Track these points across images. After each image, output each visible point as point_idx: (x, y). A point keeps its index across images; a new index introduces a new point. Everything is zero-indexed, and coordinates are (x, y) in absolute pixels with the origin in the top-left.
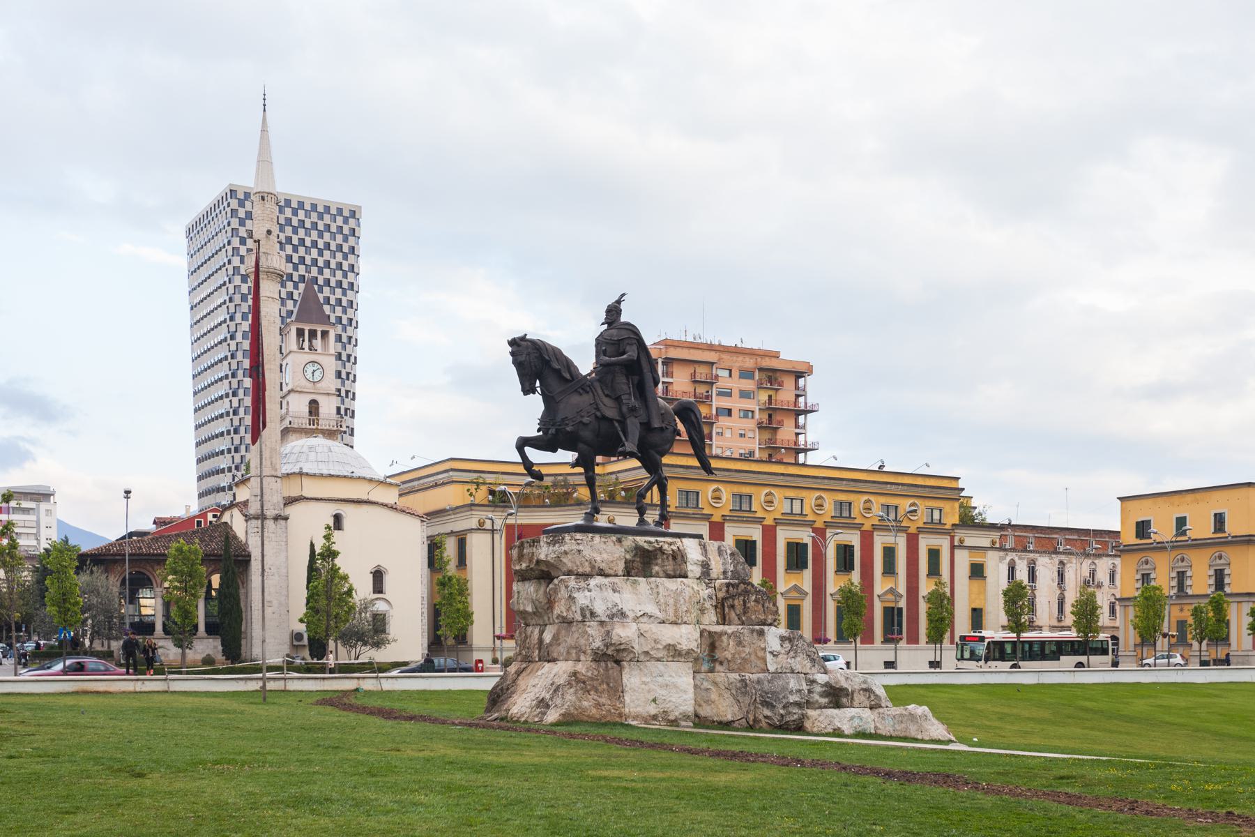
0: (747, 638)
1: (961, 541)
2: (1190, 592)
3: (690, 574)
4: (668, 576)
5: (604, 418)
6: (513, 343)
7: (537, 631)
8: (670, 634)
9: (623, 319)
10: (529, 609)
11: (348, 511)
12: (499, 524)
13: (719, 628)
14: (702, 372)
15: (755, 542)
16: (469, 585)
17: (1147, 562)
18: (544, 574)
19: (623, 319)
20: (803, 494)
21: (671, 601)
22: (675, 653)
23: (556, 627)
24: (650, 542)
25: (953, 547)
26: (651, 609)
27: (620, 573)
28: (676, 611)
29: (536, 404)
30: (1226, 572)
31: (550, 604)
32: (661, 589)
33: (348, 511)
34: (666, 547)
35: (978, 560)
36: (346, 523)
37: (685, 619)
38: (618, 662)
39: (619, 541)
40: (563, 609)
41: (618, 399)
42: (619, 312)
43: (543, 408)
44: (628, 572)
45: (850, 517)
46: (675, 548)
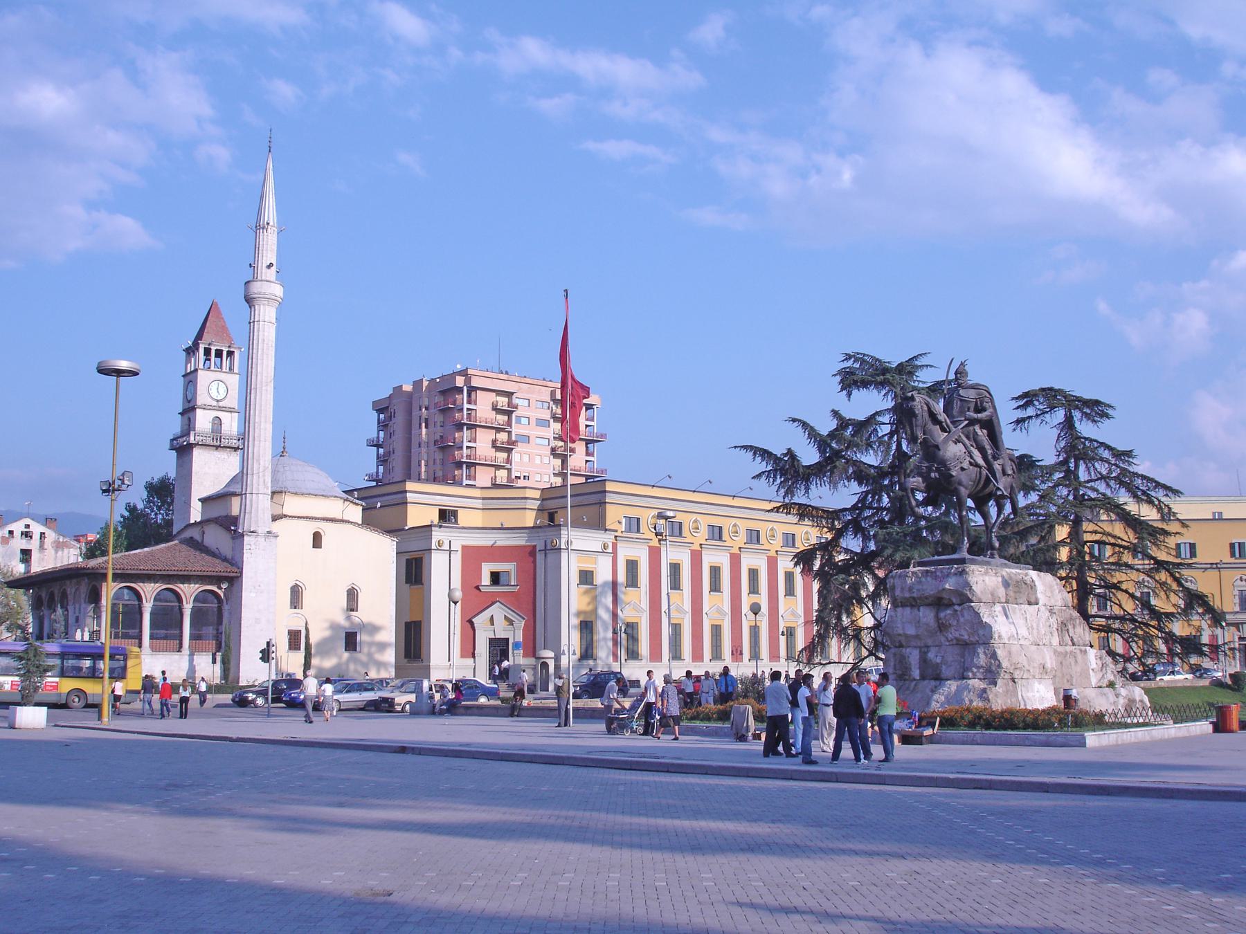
0: (1079, 656)
4: (1030, 604)
5: (974, 464)
11: (327, 530)
12: (457, 546)
13: (1061, 649)
14: (503, 402)
31: (942, 627)
41: (982, 450)
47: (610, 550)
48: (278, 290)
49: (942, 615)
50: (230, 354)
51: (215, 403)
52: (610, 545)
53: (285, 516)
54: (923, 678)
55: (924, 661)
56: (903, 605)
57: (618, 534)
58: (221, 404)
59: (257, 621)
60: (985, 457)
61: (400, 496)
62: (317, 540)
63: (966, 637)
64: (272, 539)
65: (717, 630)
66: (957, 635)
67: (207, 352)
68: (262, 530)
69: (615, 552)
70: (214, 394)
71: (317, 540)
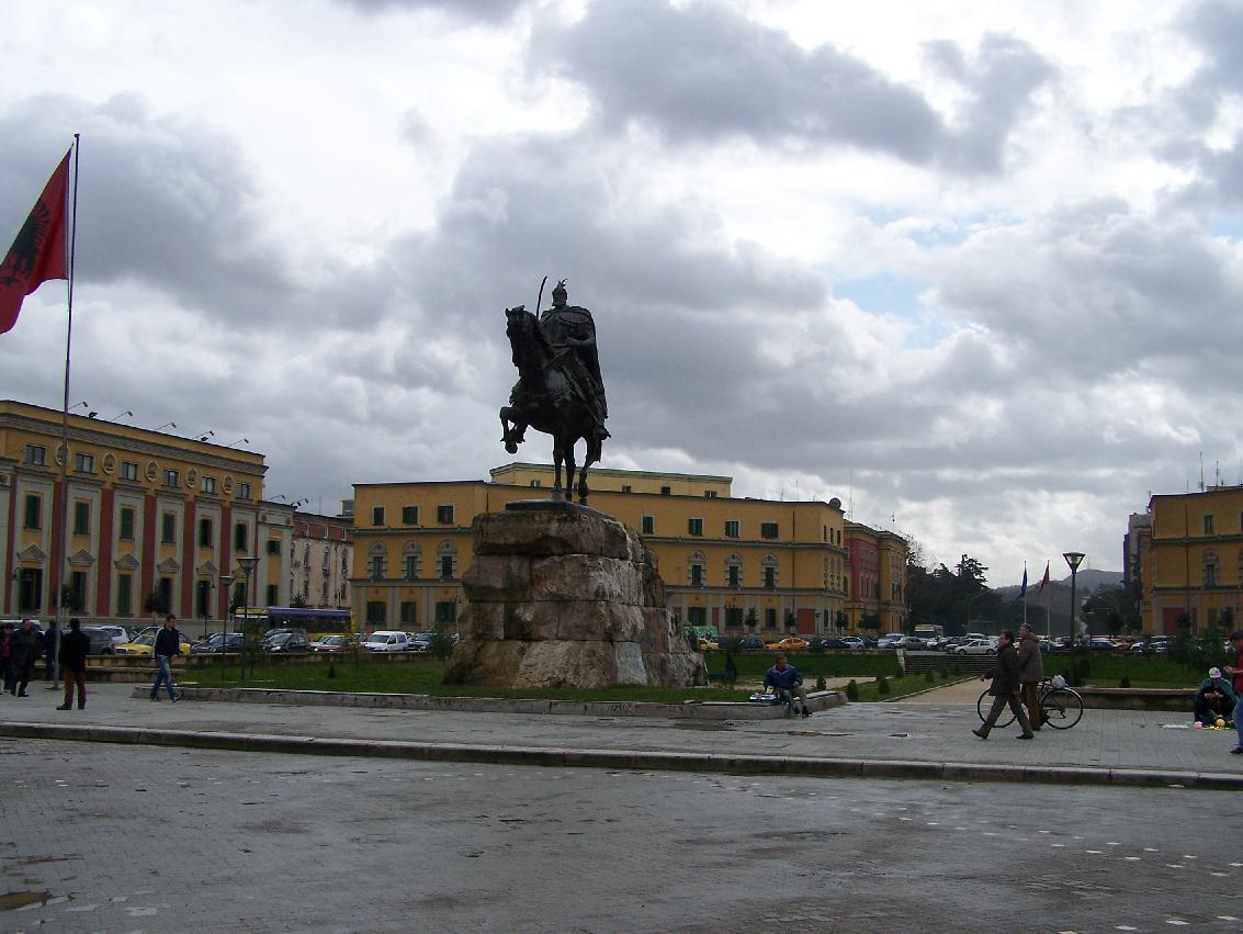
1: (264, 518)
2: (419, 576)
5: (576, 397)
7: (501, 608)
9: (570, 303)
10: (499, 584)
15: (777, 536)
16: (1104, 583)
17: (379, 547)
18: (534, 550)
19: (570, 303)
20: (139, 459)
23: (537, 605)
25: (258, 523)
30: (776, 570)
31: (535, 580)
35: (276, 537)
42: (564, 294)
45: (135, 480)
47: (8, 484)
49: (537, 566)
52: (9, 480)
54: (508, 638)
55: (511, 617)
57: (20, 465)
60: (585, 391)
65: (125, 582)
66: (554, 589)
69: (13, 490)
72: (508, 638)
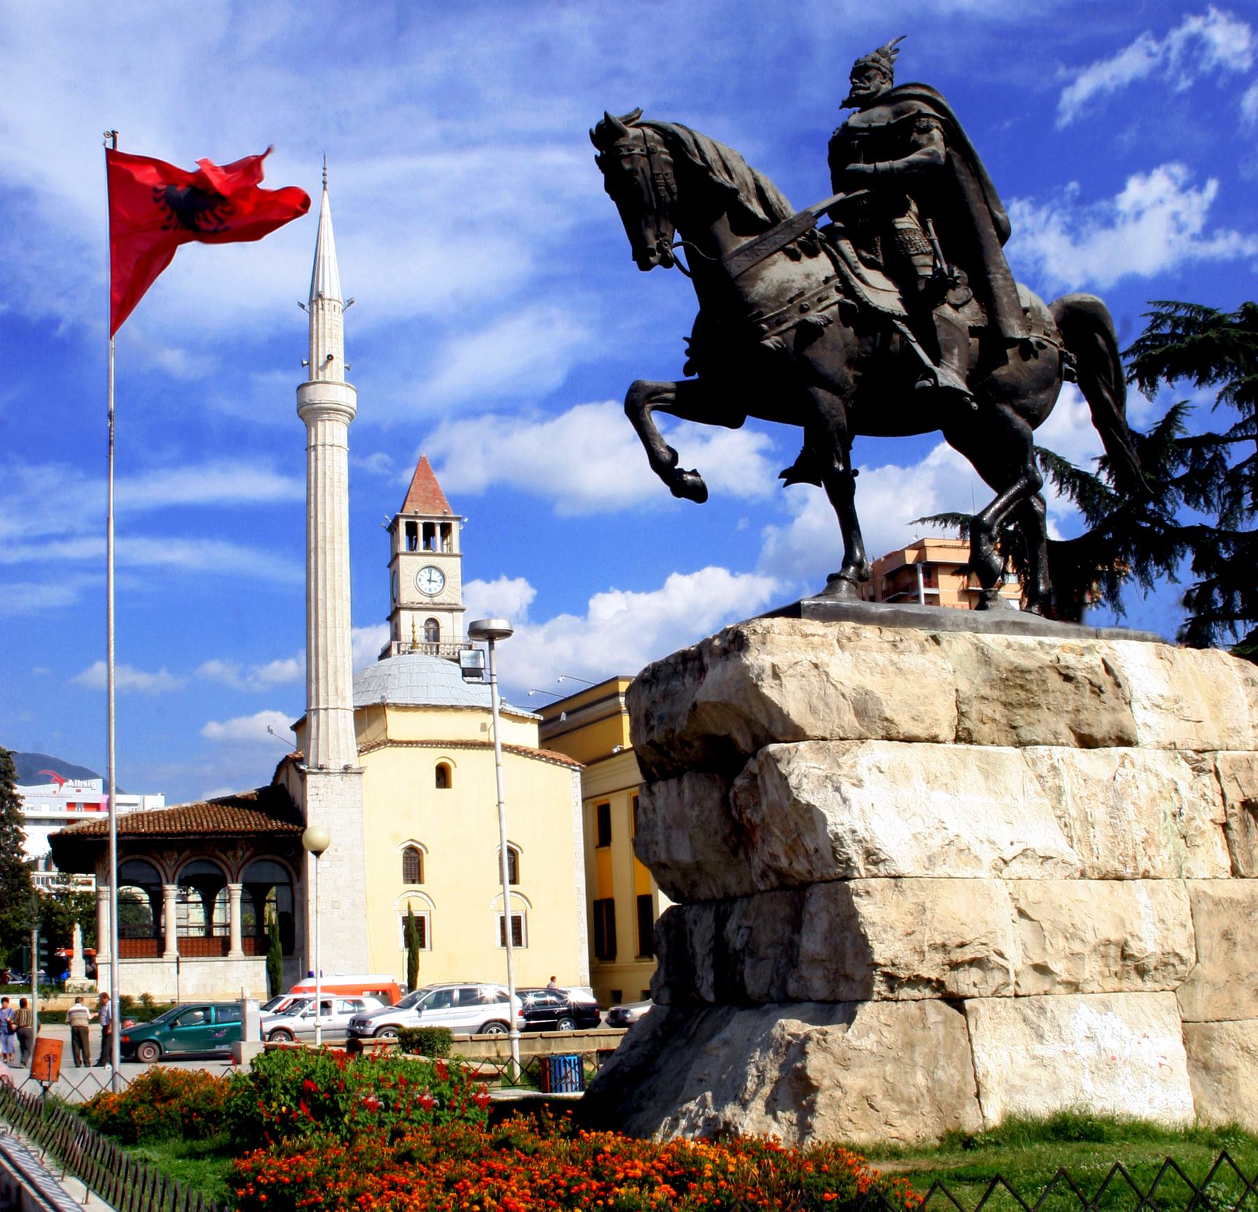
3: (1141, 735)
4: (1087, 742)
6: (606, 136)
8: (1099, 911)
21: (1099, 813)
22: (1129, 964)
24: (1022, 648)
26: (1048, 838)
27: (947, 733)
28: (1115, 839)
29: (673, 300)
32: (1068, 782)
33: (461, 762)
34: (1070, 659)
36: (455, 776)
37: (1144, 864)
38: (956, 1001)
39: (936, 640)
40: (778, 849)
41: (898, 268)
43: (698, 309)
44: (964, 737)
46: (1095, 661)
48: (346, 397)
50: (446, 529)
51: (427, 600)
53: (394, 743)
55: (719, 944)
56: (665, 777)
58: (436, 600)
59: (336, 905)
61: (611, 702)
62: (443, 776)
63: (784, 862)
64: (355, 778)
67: (411, 529)
68: (335, 765)
70: (425, 586)
71: (443, 776)
72: (719, 1003)
